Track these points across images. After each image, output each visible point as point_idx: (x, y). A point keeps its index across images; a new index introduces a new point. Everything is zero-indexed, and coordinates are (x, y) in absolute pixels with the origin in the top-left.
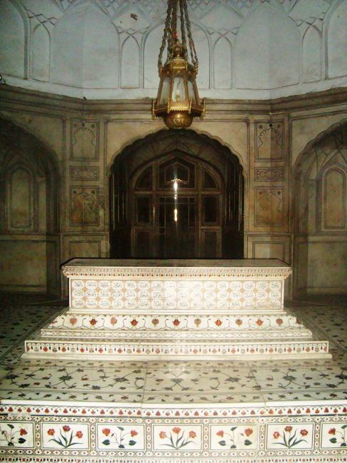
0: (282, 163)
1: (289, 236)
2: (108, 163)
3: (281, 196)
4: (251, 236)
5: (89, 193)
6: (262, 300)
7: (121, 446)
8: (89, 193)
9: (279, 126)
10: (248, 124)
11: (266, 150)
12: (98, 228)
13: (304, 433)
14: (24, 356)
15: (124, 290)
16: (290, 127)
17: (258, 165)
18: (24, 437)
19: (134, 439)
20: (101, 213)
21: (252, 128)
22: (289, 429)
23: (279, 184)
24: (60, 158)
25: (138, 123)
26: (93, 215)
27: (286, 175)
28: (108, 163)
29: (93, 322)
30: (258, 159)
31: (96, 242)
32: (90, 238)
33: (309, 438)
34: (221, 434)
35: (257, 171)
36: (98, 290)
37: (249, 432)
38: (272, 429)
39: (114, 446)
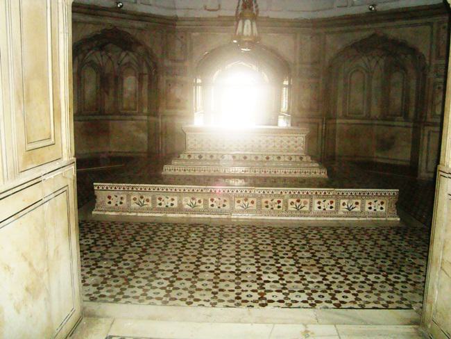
7: (219, 207)
13: (305, 203)
14: (163, 173)
18: (173, 202)
19: (225, 204)
22: (298, 201)
29: (200, 157)
33: (308, 206)
34: (267, 202)
37: (279, 202)
38: (290, 200)
39: (216, 207)
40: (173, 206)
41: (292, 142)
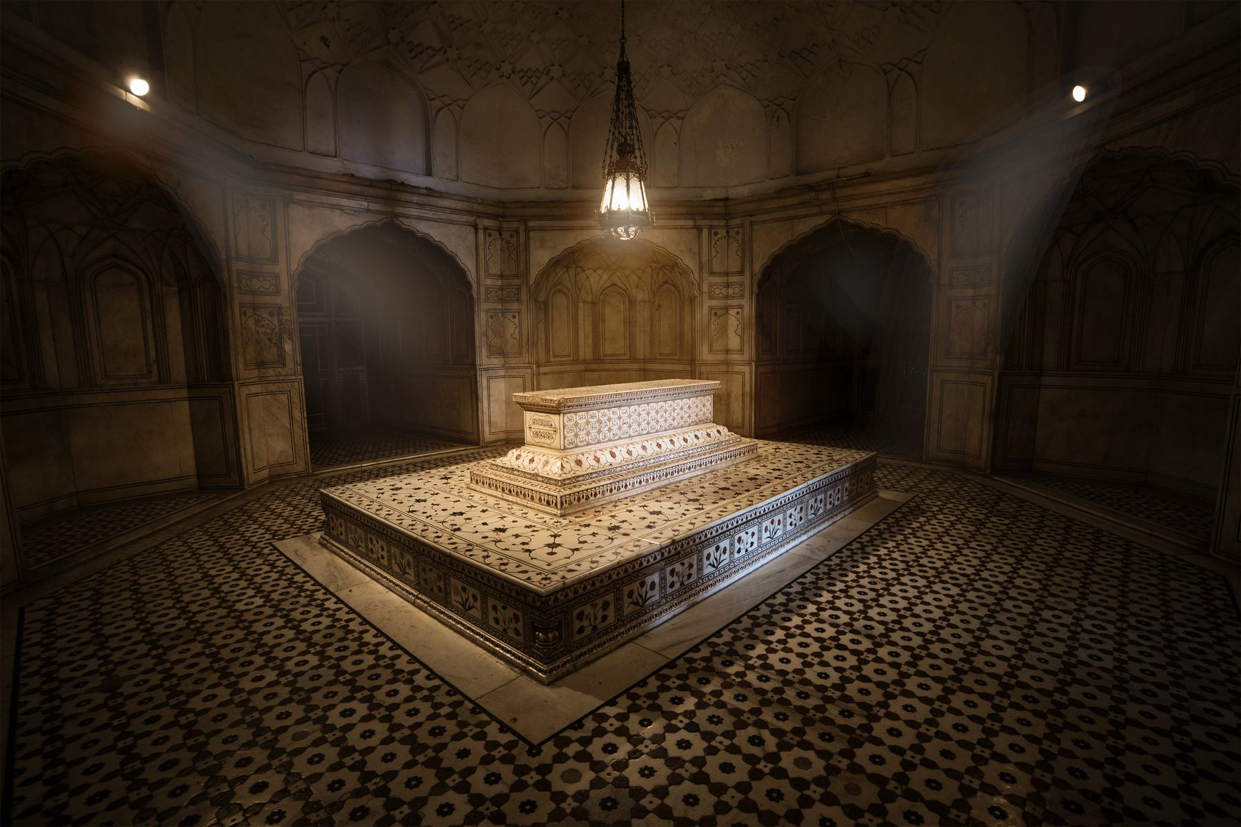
0: (517, 282)
1: (531, 368)
2: (294, 267)
3: (517, 320)
4: (486, 370)
5: (266, 315)
6: (701, 416)
8: (266, 315)
9: (512, 236)
10: (476, 230)
11: (495, 269)
12: (284, 372)
15: (609, 419)
16: (527, 238)
17: (488, 282)
20: (288, 347)
21: (481, 235)
23: (515, 306)
24: (224, 257)
25: (338, 212)
26: (275, 349)
27: (524, 296)
28: (294, 267)
30: (488, 275)
31: (281, 392)
32: (272, 388)
35: (487, 288)
36: (588, 423)
40: (692, 580)
41: (700, 406)
